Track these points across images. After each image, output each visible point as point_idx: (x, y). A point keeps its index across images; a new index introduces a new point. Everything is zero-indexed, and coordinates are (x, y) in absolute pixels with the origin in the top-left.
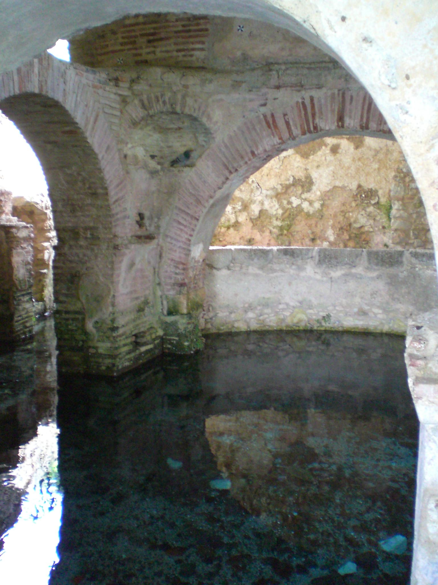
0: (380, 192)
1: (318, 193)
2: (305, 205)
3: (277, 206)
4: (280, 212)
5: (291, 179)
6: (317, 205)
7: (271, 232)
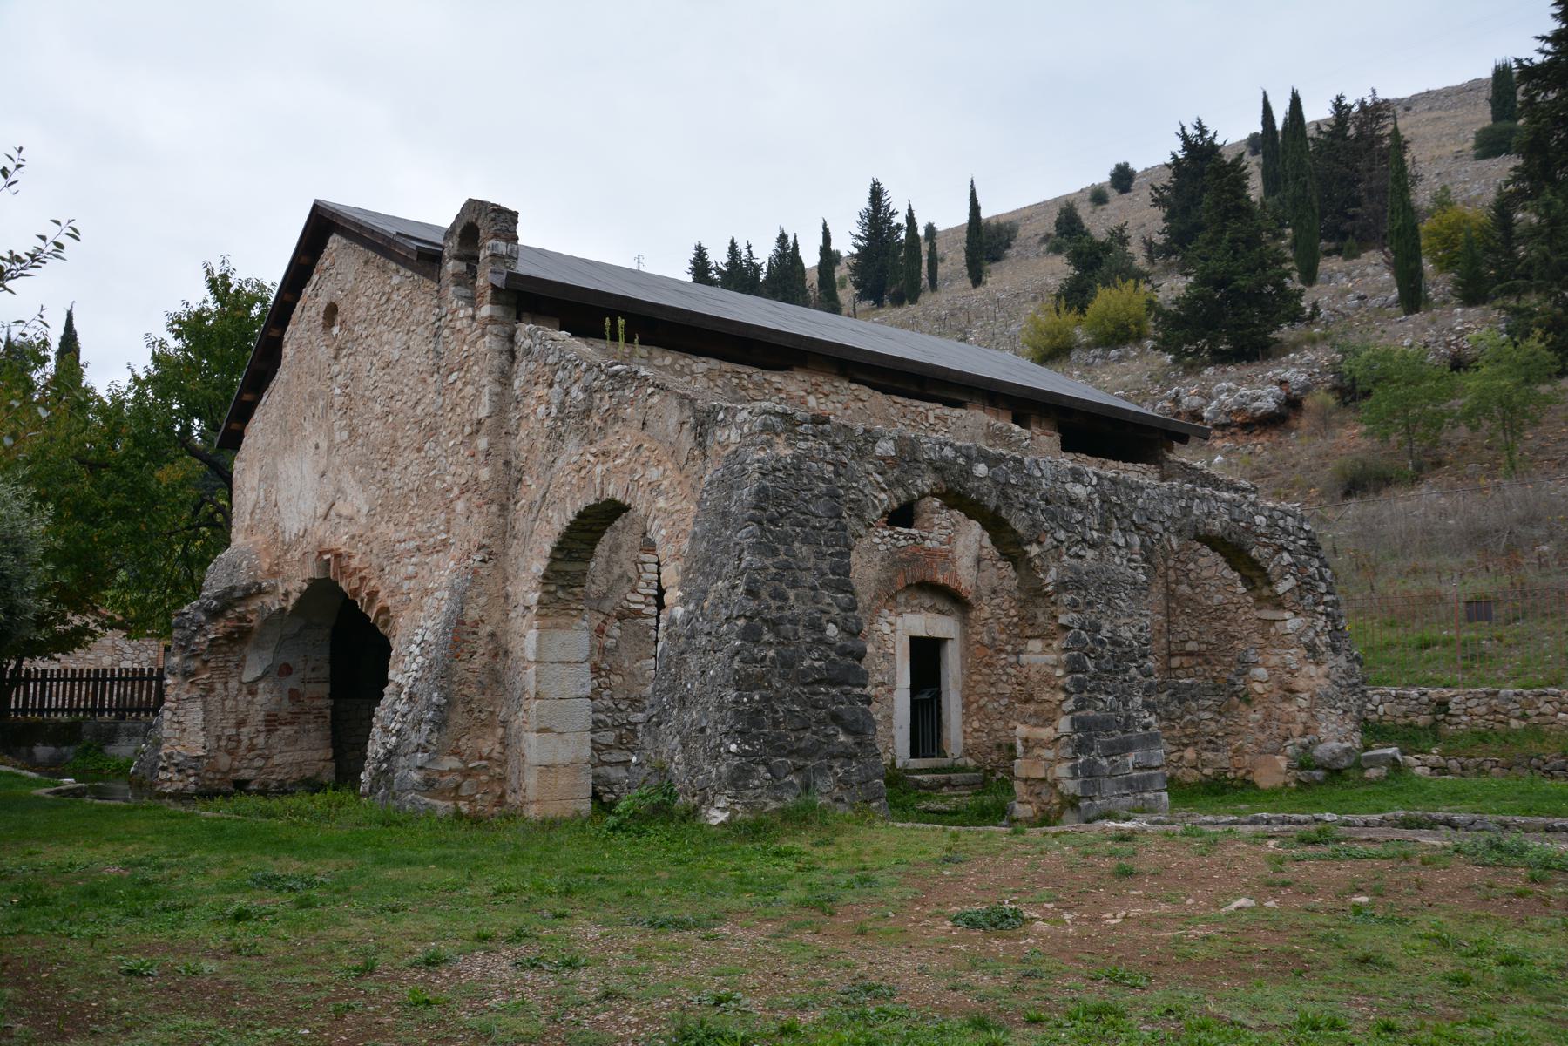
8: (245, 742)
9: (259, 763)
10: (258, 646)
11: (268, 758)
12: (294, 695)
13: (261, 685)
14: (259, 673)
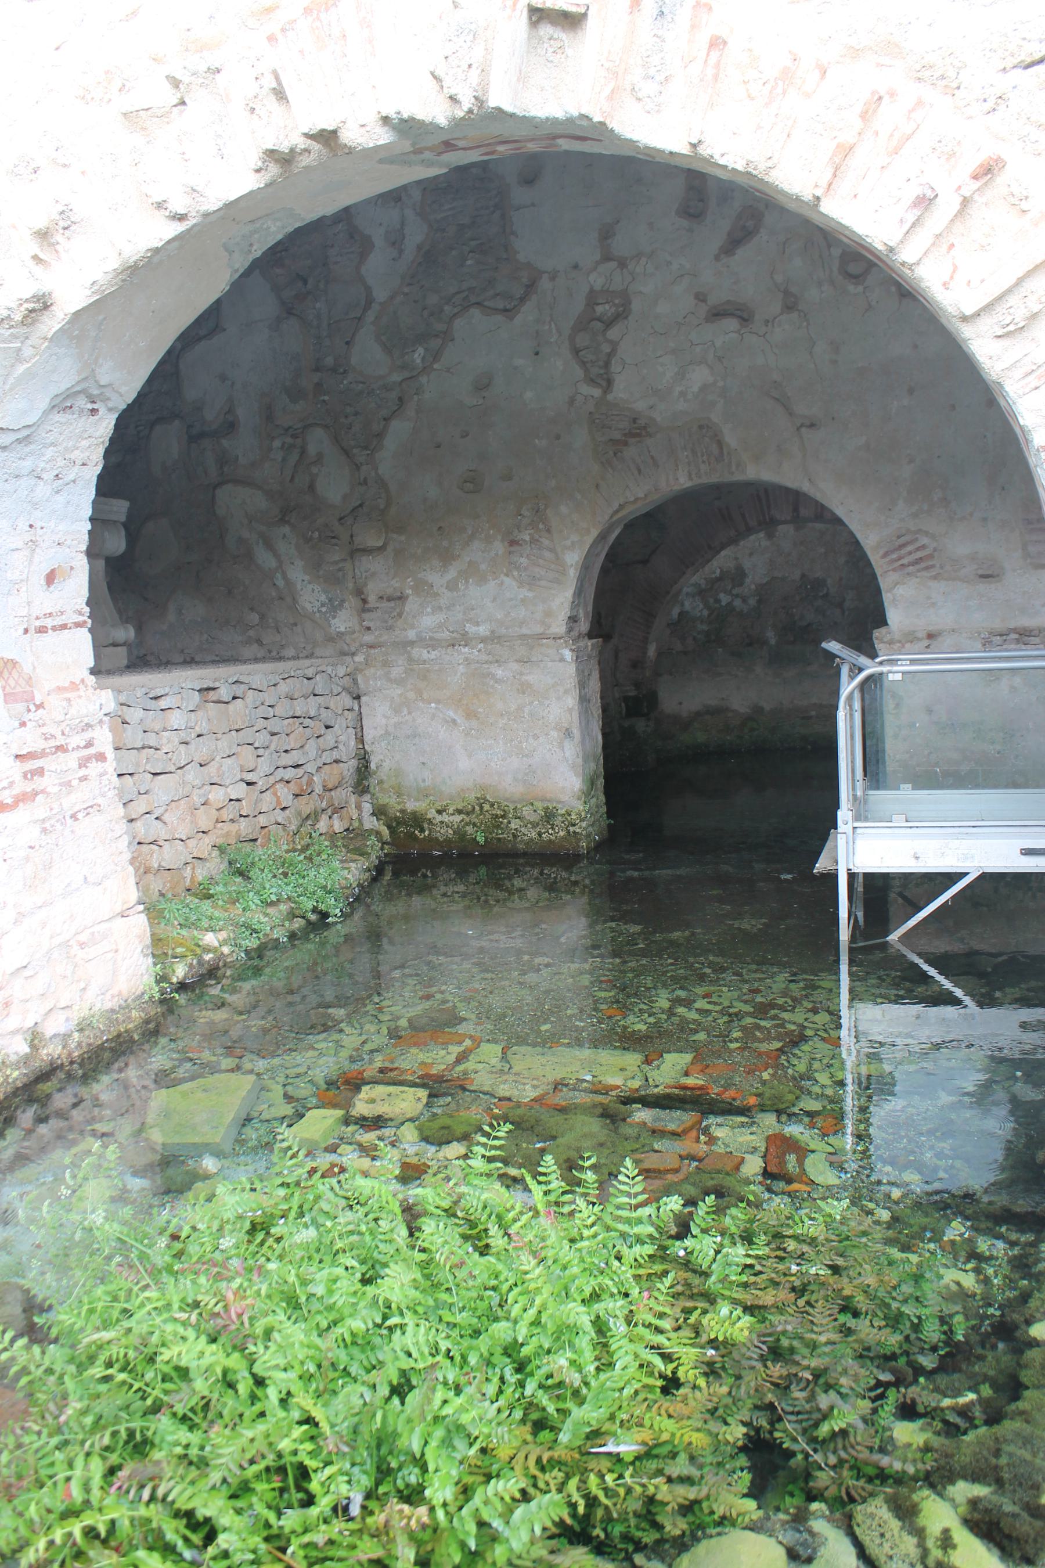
0: (829, 581)
1: (753, 587)
2: (738, 603)
3: (701, 606)
4: (706, 613)
5: (718, 571)
6: (752, 602)
7: (694, 639)
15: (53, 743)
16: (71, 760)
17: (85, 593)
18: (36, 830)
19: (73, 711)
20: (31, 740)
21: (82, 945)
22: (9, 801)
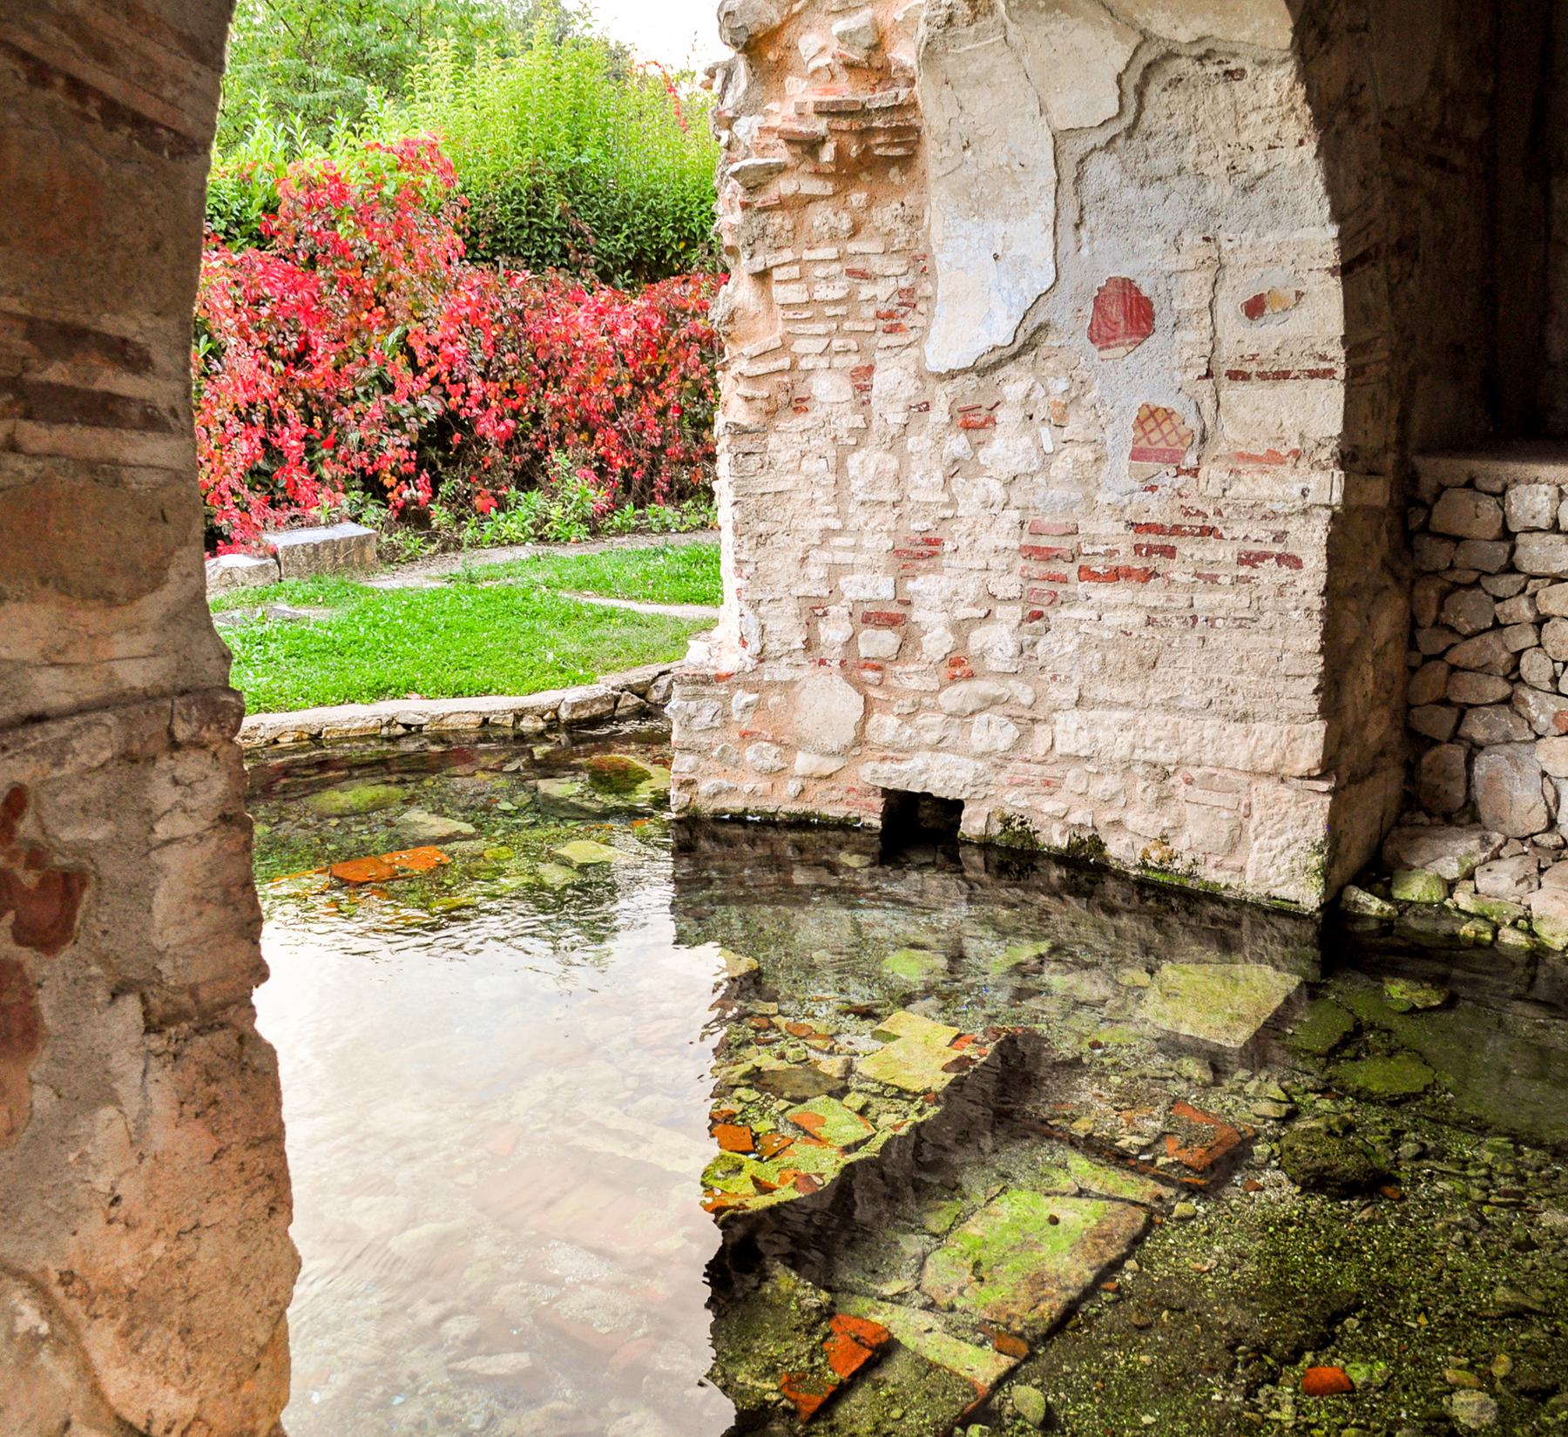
8: (936, 642)
9: (994, 733)
10: (977, 206)
11: (1028, 722)
12: (1159, 439)
13: (1015, 385)
14: (1001, 331)
15: (1199, 521)
16: (1225, 552)
17: (1336, 327)
18: (1139, 618)
19: (1239, 489)
20: (1157, 509)
21: (1189, 782)
22: (1100, 569)
